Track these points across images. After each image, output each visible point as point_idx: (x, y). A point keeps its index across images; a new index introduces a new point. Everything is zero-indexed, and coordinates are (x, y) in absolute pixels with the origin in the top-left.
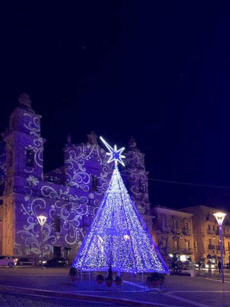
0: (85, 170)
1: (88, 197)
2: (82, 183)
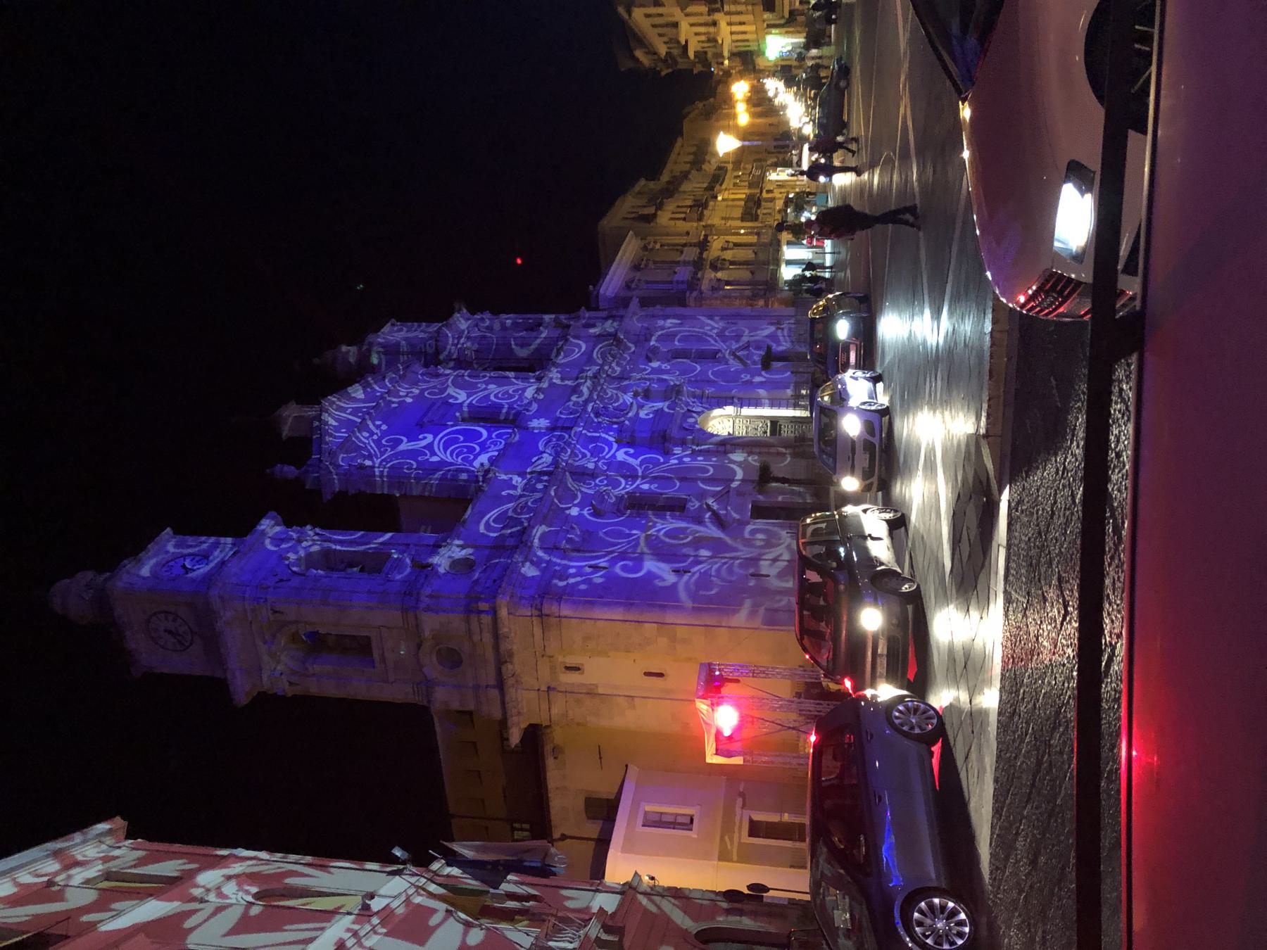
1: (541, 435)
2: (481, 444)
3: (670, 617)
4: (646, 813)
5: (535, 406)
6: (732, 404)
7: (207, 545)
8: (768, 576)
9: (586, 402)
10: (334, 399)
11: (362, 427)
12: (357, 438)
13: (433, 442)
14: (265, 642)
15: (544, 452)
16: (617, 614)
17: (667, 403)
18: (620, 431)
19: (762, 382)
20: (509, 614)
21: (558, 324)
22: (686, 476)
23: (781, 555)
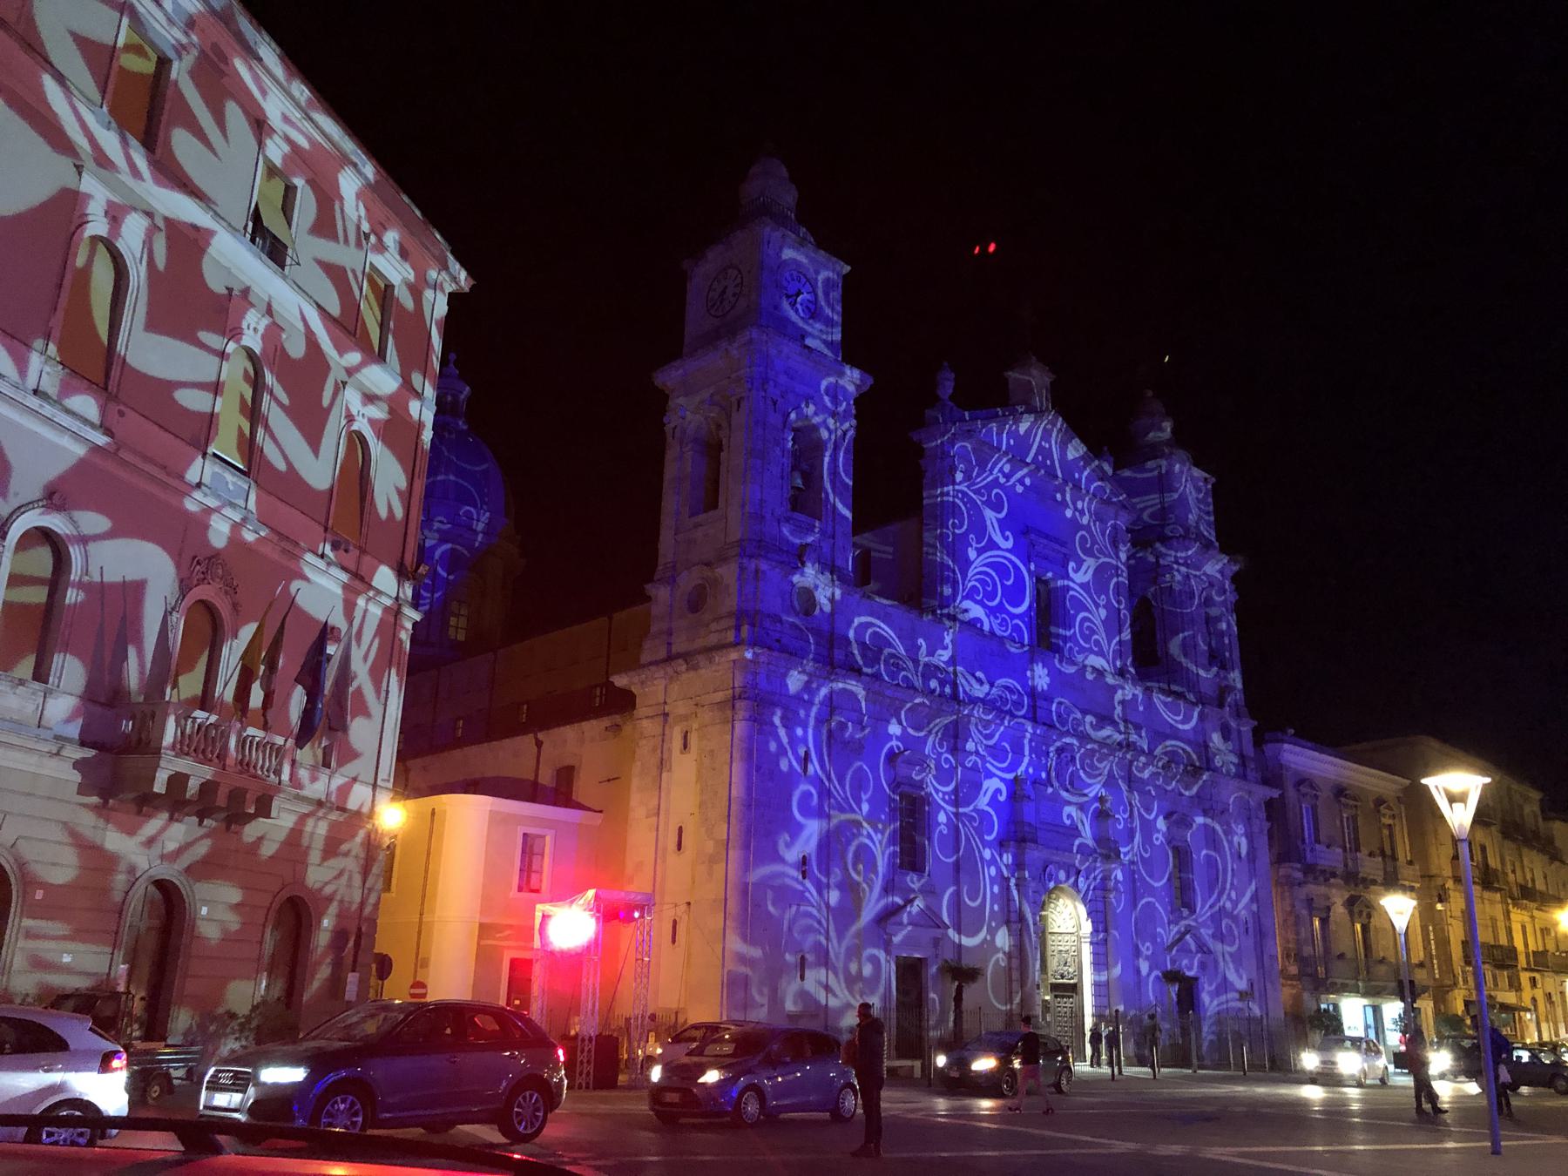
0: (1009, 544)
1: (1023, 680)
2: (1000, 607)
3: (735, 855)
4: (544, 837)
5: (1071, 670)
6: (1095, 931)
7: (830, 314)
8: (802, 978)
9: (1084, 738)
11: (1018, 460)
12: (999, 459)
14: (712, 395)
15: (992, 685)
16: (737, 791)
17: (1090, 842)
18: (1036, 781)
19: (1138, 971)
20: (734, 661)
21: (1224, 690)
22: (964, 870)
23: (835, 995)
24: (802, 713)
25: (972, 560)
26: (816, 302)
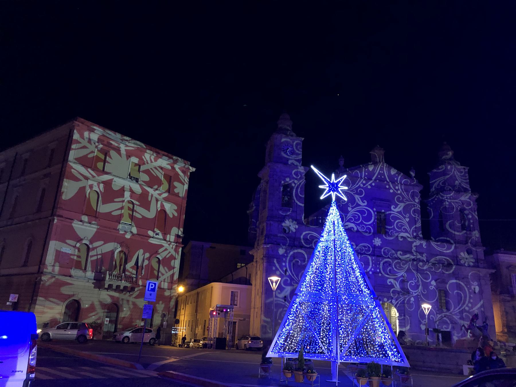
0: (366, 204)
1: (371, 243)
2: (362, 223)
6: (400, 315)
10: (385, 165)
13: (361, 206)
24: (284, 259)
25: (349, 210)
26: (293, 150)
